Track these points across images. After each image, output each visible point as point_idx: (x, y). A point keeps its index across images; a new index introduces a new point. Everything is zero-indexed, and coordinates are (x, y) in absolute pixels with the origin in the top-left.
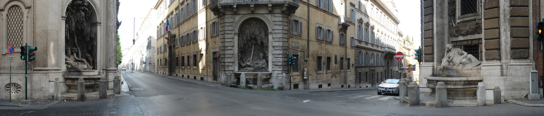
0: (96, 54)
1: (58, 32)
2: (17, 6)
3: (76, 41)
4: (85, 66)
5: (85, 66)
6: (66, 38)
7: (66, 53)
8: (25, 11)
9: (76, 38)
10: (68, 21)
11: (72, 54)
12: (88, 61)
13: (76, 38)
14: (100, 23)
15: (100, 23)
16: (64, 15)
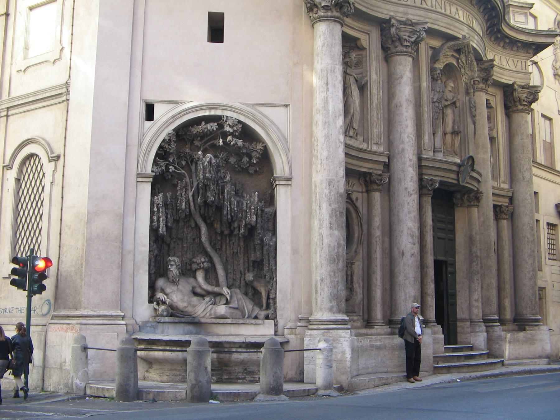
0: (273, 272)
1: (123, 216)
2: (37, 156)
3: (204, 238)
4: (222, 309)
5: (222, 309)
6: (154, 231)
7: (158, 270)
8: (48, 167)
9: (204, 229)
10: (160, 183)
11: (188, 271)
12: (253, 294)
13: (204, 229)
14: (289, 179)
15: (289, 179)
16: (149, 169)
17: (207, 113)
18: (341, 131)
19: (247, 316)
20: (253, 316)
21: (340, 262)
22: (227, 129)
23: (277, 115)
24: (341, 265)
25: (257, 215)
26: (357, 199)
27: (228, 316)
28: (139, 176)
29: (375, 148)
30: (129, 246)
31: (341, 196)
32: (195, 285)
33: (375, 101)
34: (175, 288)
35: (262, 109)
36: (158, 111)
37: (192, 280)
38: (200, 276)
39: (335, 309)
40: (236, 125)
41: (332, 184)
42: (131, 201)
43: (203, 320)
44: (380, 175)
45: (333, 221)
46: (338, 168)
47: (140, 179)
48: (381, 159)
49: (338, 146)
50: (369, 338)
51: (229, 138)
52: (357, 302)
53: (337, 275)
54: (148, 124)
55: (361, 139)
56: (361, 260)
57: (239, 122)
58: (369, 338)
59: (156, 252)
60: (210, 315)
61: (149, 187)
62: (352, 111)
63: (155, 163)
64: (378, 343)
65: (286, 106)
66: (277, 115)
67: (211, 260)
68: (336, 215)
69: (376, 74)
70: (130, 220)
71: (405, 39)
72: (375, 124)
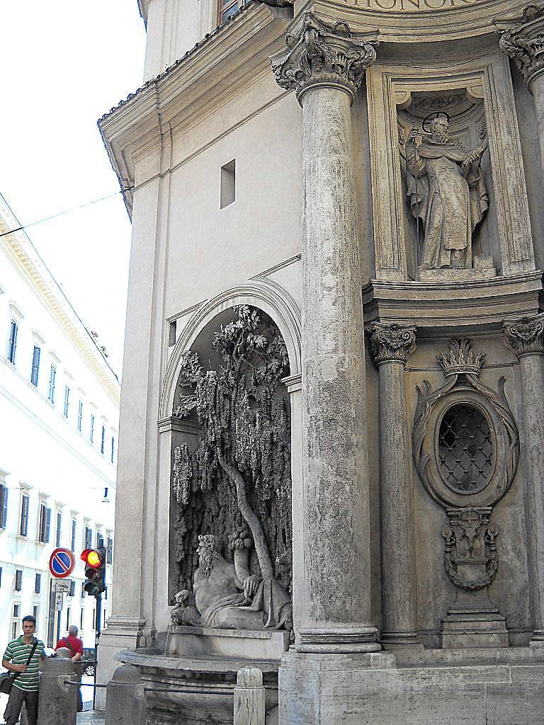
6: (173, 496)
17: (219, 310)
18: (327, 267)
19: (267, 625)
20: (278, 625)
21: (327, 517)
22: (240, 324)
23: (289, 279)
24: (328, 523)
25: (259, 454)
26: (502, 380)
27: (230, 623)
28: (160, 424)
29: (515, 270)
30: (150, 526)
31: (328, 387)
32: (232, 575)
33: (512, 181)
34: (203, 582)
35: (273, 277)
36: (182, 324)
37: (229, 567)
38: (238, 559)
39: (318, 613)
40: (250, 315)
41: (310, 372)
42: (153, 460)
43: (206, 632)
44: (525, 321)
45: (313, 441)
46: (321, 337)
47: (161, 429)
48: (524, 288)
49: (321, 296)
50: (462, 671)
51: (249, 338)
52: (515, 589)
53: (320, 544)
54: (171, 349)
55: (488, 262)
56: (521, 502)
57: (251, 308)
58: (462, 671)
59: (184, 530)
60: (215, 624)
61: (169, 436)
62: (437, 220)
63: (178, 402)
64: (497, 682)
65: (299, 257)
66: (289, 279)
67: (249, 536)
68: (318, 427)
69: (510, 133)
70: (152, 488)
71: (533, 46)
72: (515, 224)
